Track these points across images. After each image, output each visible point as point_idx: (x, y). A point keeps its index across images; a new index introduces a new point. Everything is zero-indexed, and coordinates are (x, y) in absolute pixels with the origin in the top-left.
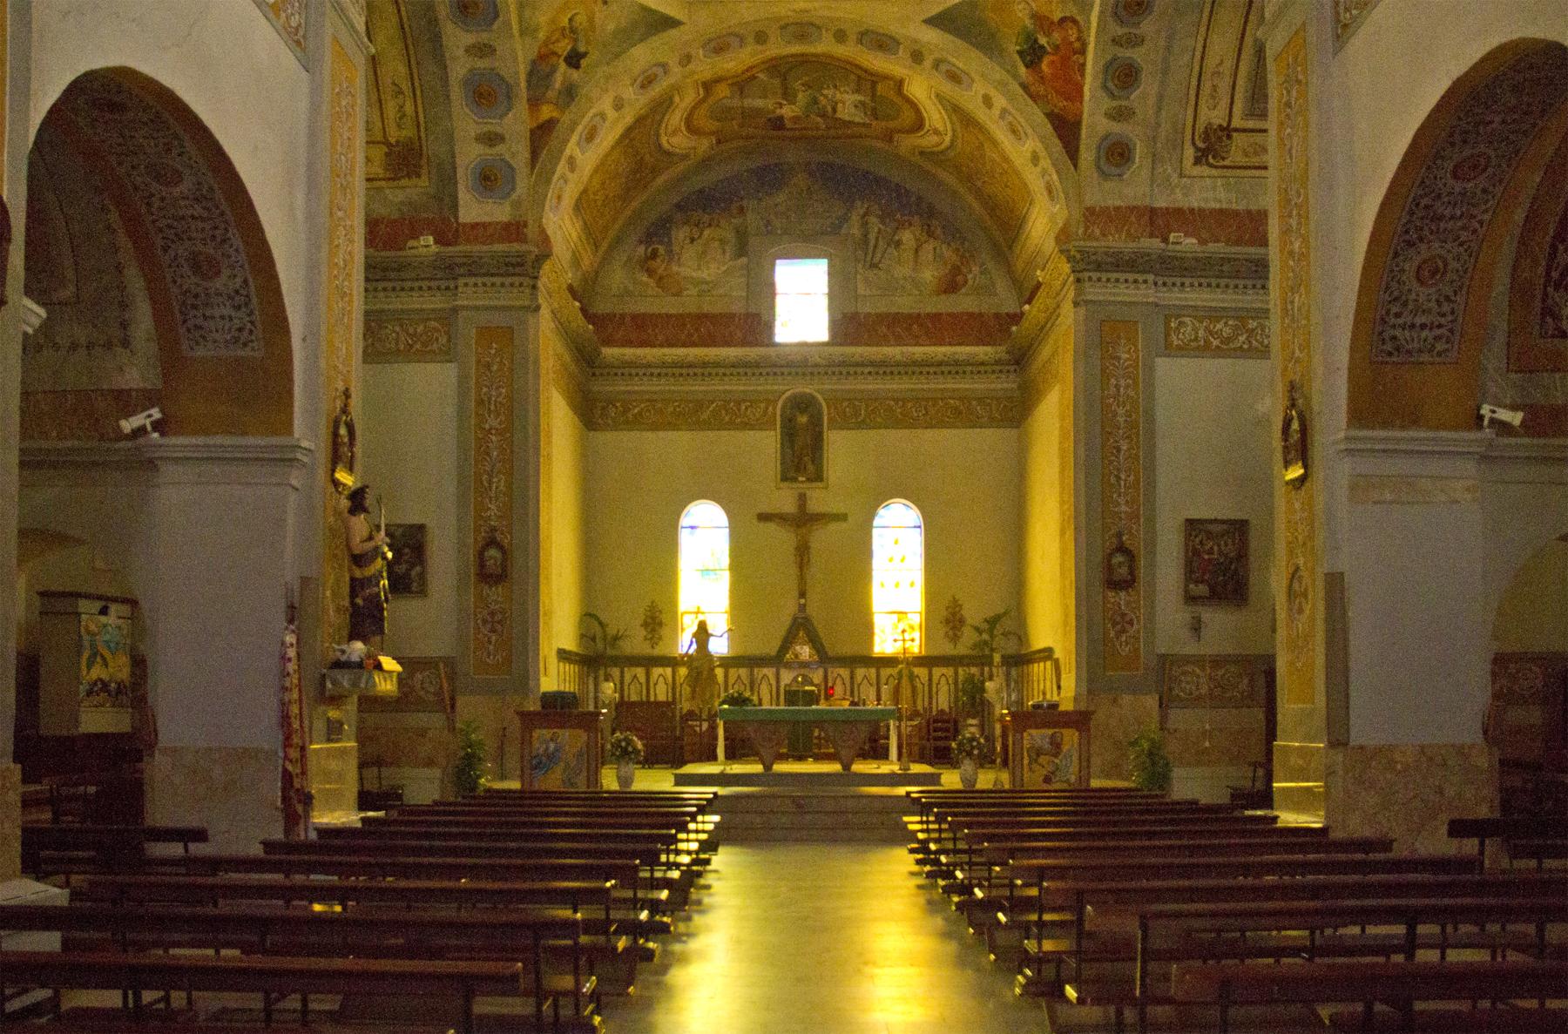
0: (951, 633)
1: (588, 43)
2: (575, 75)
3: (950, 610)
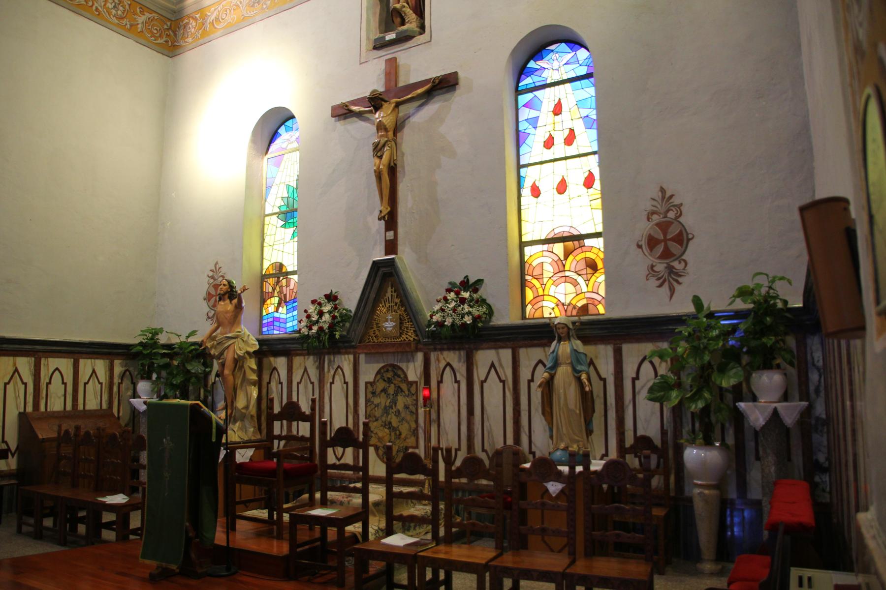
0: (660, 267)
3: (655, 217)
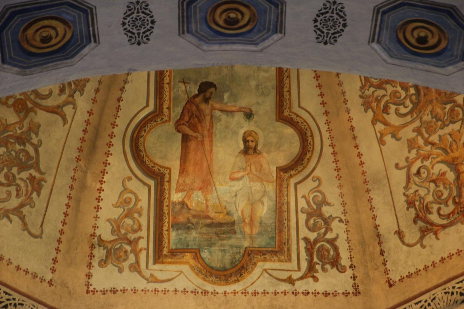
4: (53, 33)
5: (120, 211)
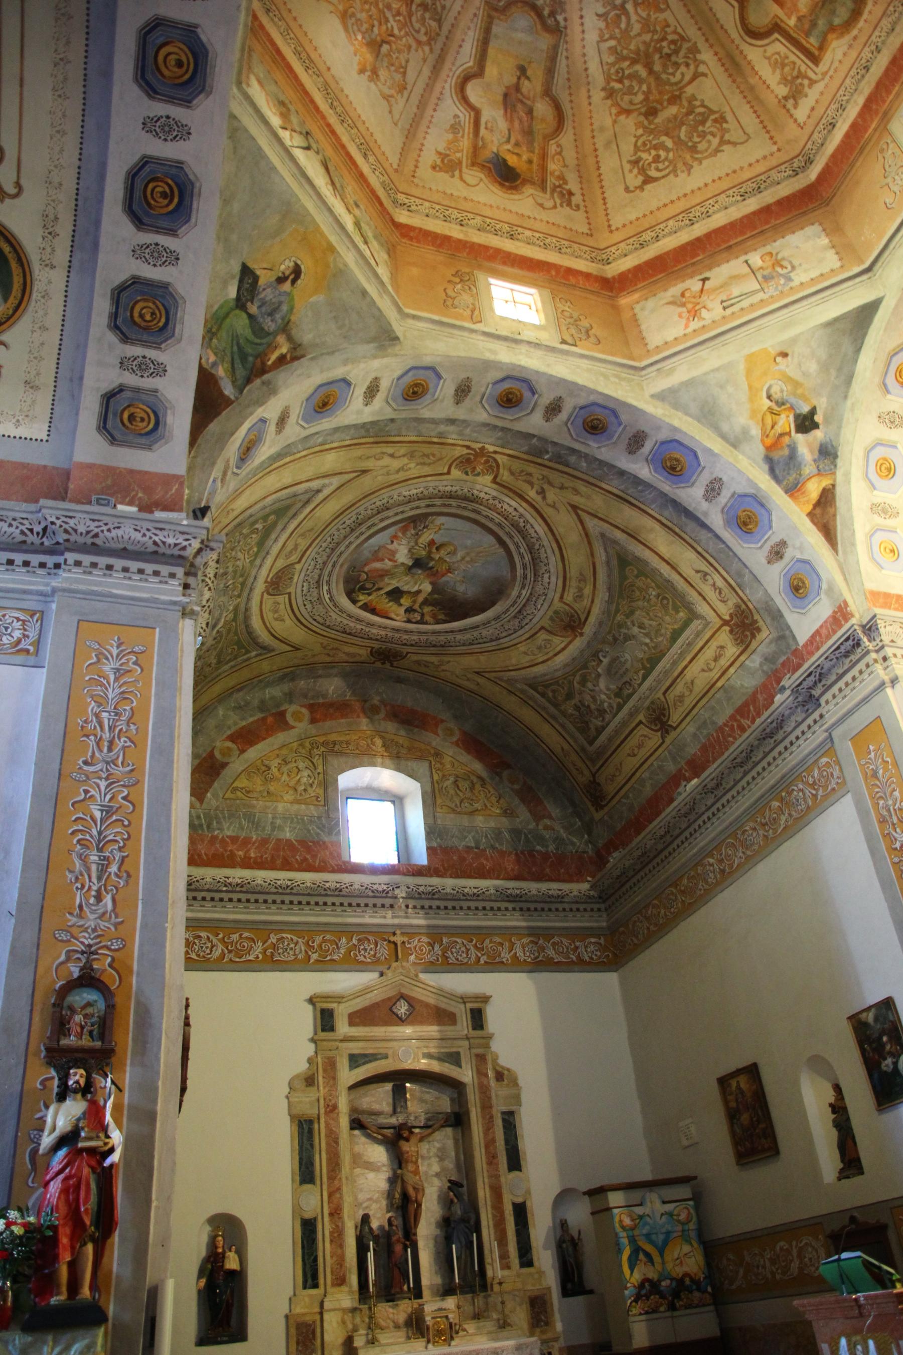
1: (805, 399)
2: (818, 435)
4: (173, 57)
5: (778, 71)
